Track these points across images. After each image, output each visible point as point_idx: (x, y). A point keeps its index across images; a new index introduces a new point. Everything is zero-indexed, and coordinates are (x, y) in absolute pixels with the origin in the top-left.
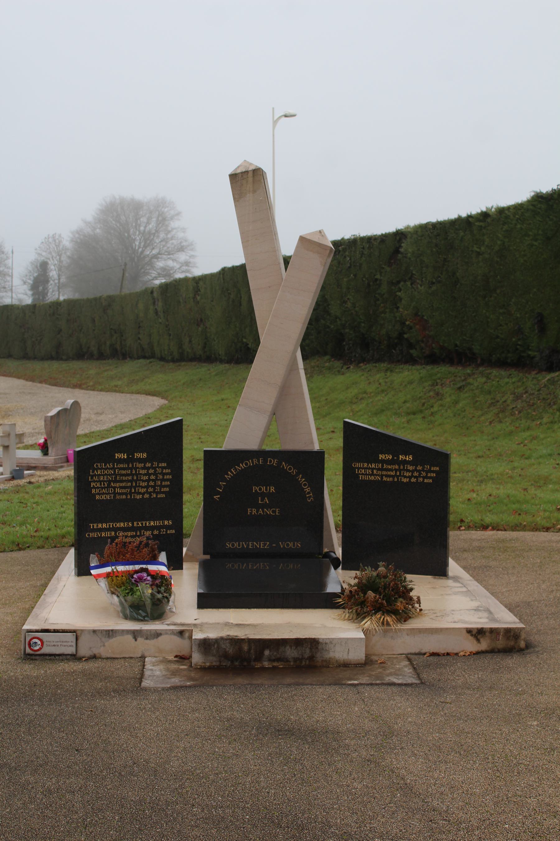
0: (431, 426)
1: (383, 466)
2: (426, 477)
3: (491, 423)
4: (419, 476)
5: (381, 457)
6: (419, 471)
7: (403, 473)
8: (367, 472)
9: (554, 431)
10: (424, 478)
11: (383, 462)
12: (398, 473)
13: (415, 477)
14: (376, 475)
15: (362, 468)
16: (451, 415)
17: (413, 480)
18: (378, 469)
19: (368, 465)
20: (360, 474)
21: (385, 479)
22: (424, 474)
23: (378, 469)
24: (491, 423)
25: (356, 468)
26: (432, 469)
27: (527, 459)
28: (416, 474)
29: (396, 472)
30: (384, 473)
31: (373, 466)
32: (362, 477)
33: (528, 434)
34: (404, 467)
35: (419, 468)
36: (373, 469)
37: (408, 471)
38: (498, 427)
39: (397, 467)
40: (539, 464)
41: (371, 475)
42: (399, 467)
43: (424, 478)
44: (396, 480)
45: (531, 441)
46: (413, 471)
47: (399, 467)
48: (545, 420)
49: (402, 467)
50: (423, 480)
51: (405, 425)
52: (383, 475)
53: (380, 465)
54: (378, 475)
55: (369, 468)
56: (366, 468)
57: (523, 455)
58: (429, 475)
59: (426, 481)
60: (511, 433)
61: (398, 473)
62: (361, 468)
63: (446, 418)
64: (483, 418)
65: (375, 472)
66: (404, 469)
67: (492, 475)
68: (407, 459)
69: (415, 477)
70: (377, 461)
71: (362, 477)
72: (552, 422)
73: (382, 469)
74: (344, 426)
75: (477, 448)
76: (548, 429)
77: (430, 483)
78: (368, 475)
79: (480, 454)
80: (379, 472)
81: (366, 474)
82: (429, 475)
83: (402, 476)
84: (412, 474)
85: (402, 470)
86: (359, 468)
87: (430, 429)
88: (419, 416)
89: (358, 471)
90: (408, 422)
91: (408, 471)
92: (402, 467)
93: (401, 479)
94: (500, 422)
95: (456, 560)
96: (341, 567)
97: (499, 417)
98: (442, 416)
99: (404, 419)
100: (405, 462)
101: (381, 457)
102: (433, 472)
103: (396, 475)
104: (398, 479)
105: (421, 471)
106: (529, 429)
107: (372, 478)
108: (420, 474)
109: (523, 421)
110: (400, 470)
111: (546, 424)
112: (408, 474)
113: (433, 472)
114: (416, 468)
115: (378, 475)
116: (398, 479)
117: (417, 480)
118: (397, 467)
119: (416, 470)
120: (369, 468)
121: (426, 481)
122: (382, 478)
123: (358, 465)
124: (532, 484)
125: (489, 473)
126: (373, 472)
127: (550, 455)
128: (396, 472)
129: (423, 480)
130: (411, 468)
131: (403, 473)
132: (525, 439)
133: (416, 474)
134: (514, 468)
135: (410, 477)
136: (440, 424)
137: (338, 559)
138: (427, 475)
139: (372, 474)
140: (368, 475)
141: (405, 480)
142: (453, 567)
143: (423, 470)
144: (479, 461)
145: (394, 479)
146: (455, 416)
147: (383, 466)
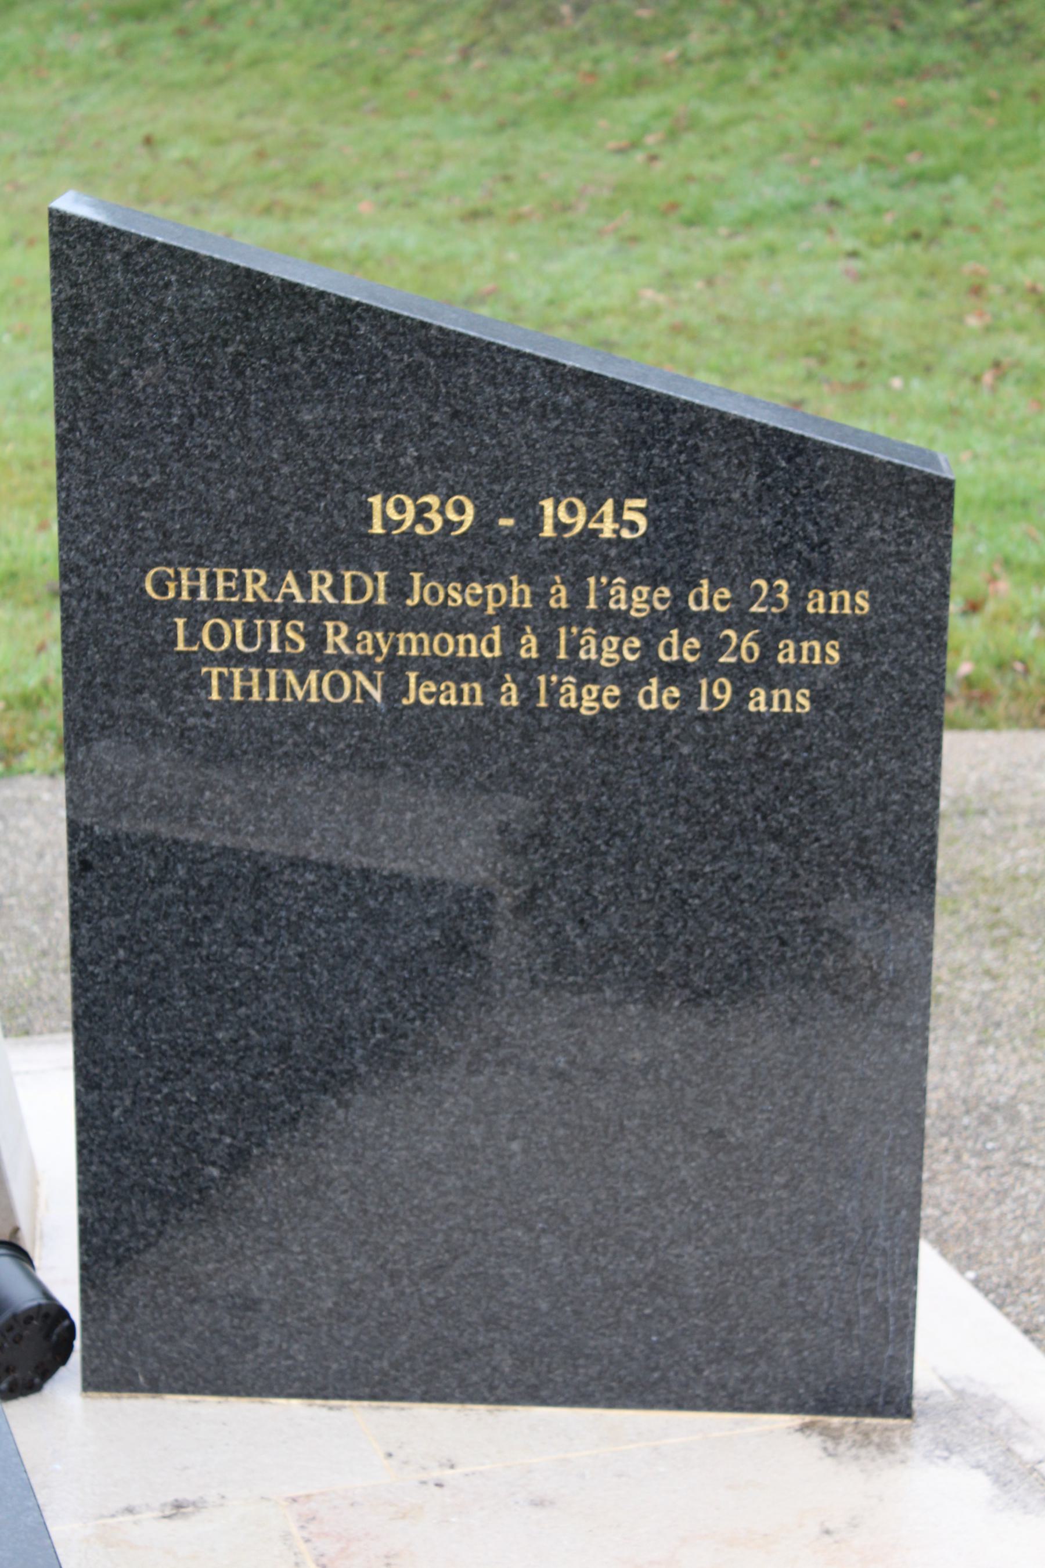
0: (219, 69)
1: (399, 589)
2: (766, 672)
3: (466, 55)
4: (709, 666)
5: (386, 512)
6: (704, 626)
7: (573, 649)
8: (260, 636)
9: (753, 91)
10: (744, 677)
11: (403, 554)
12: (529, 647)
13: (675, 673)
14: (348, 665)
15: (230, 612)
16: (294, 22)
17: (657, 697)
18: (367, 617)
19: (274, 584)
20: (210, 659)
21: (419, 692)
22: (746, 647)
23: (367, 617)
24: (466, 55)
25: (173, 608)
26: (816, 603)
27: (690, 223)
28: (679, 648)
29: (512, 637)
30: (413, 643)
31: (321, 591)
32: (226, 683)
33: (647, 104)
34: (579, 596)
35: (708, 598)
36: (316, 616)
37: (612, 622)
38: (510, 71)
39: (518, 594)
40: (771, 251)
41: (302, 665)
42: (541, 596)
43: (744, 677)
44: (511, 696)
45: (672, 136)
46: (650, 630)
47: (541, 596)
48: (698, 42)
49: (560, 597)
50: (741, 696)
51: (114, 65)
52: (407, 662)
53: (378, 587)
54: (365, 663)
55: (287, 612)
56: (262, 610)
57: (673, 207)
58: (787, 654)
59: (758, 701)
60: (569, 102)
61: (529, 647)
62: (213, 608)
63: (273, 35)
64: (427, 35)
65: (336, 637)
66: (576, 614)
67: (589, 316)
68: (608, 529)
69: (675, 673)
70: (349, 547)
71: (226, 683)
72: (732, 53)
73: (395, 618)
74: (57, 259)
75: (449, 171)
76: (723, 80)
77: (796, 720)
78: (281, 661)
79: (475, 198)
80: (372, 641)
81: (262, 659)
82: (787, 654)
83: (565, 668)
84: (648, 648)
85: (555, 616)
86: (195, 613)
87: (220, 82)
88: (166, 26)
89: (193, 638)
90: (123, 50)
91: (612, 622)
92: (560, 597)
93: (553, 693)
94: (505, 50)
95: (941, 1244)
96: (76, 1358)
97: (492, 31)
98: (255, 24)
99: (105, 40)
100: (583, 555)
101: (386, 512)
102: (825, 628)
103: (510, 662)
104: (528, 692)
105: (725, 621)
106: (640, 82)
107: (313, 688)
108: (713, 647)
109: (606, 47)
110: (548, 621)
111: (708, 58)
112: (611, 651)
113: (825, 628)
114: (679, 597)
115: (365, 663)
116: (528, 692)
117: (690, 698)
118: (518, 594)
119: (681, 617)
120: (287, 612)
121: (758, 701)
122: (395, 687)
123: (187, 583)
124: (810, 377)
125: (572, 310)
126: (316, 639)
127: (798, 208)
128: (512, 637)
129: (741, 696)
130: (640, 601)
131: (573, 649)
132: (646, 129)
133: (679, 648)
134: (669, 280)
135: (629, 677)
136: (254, 63)
137: (52, 1314)
138: (769, 651)
139: (316, 658)
140: (281, 661)
141: (590, 701)
142: (953, 1328)
143: (741, 620)
144: (486, 234)
145: (493, 688)
146: (307, 24)
147: (399, 589)
